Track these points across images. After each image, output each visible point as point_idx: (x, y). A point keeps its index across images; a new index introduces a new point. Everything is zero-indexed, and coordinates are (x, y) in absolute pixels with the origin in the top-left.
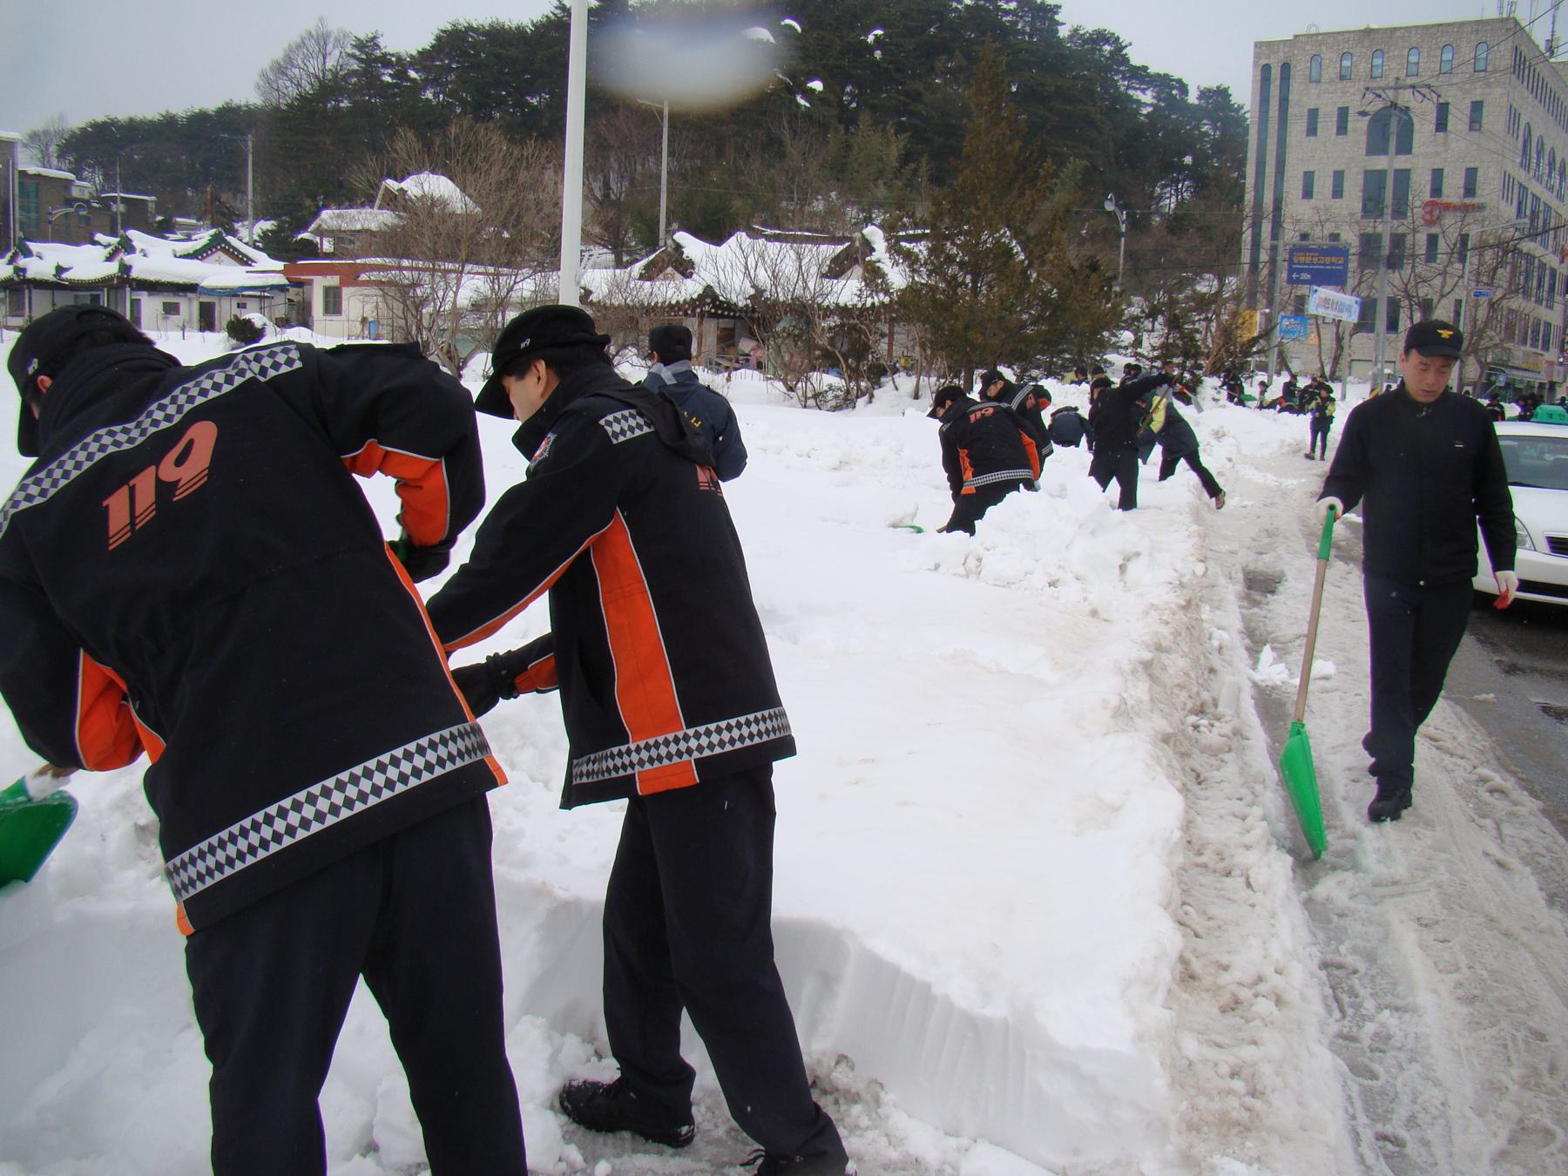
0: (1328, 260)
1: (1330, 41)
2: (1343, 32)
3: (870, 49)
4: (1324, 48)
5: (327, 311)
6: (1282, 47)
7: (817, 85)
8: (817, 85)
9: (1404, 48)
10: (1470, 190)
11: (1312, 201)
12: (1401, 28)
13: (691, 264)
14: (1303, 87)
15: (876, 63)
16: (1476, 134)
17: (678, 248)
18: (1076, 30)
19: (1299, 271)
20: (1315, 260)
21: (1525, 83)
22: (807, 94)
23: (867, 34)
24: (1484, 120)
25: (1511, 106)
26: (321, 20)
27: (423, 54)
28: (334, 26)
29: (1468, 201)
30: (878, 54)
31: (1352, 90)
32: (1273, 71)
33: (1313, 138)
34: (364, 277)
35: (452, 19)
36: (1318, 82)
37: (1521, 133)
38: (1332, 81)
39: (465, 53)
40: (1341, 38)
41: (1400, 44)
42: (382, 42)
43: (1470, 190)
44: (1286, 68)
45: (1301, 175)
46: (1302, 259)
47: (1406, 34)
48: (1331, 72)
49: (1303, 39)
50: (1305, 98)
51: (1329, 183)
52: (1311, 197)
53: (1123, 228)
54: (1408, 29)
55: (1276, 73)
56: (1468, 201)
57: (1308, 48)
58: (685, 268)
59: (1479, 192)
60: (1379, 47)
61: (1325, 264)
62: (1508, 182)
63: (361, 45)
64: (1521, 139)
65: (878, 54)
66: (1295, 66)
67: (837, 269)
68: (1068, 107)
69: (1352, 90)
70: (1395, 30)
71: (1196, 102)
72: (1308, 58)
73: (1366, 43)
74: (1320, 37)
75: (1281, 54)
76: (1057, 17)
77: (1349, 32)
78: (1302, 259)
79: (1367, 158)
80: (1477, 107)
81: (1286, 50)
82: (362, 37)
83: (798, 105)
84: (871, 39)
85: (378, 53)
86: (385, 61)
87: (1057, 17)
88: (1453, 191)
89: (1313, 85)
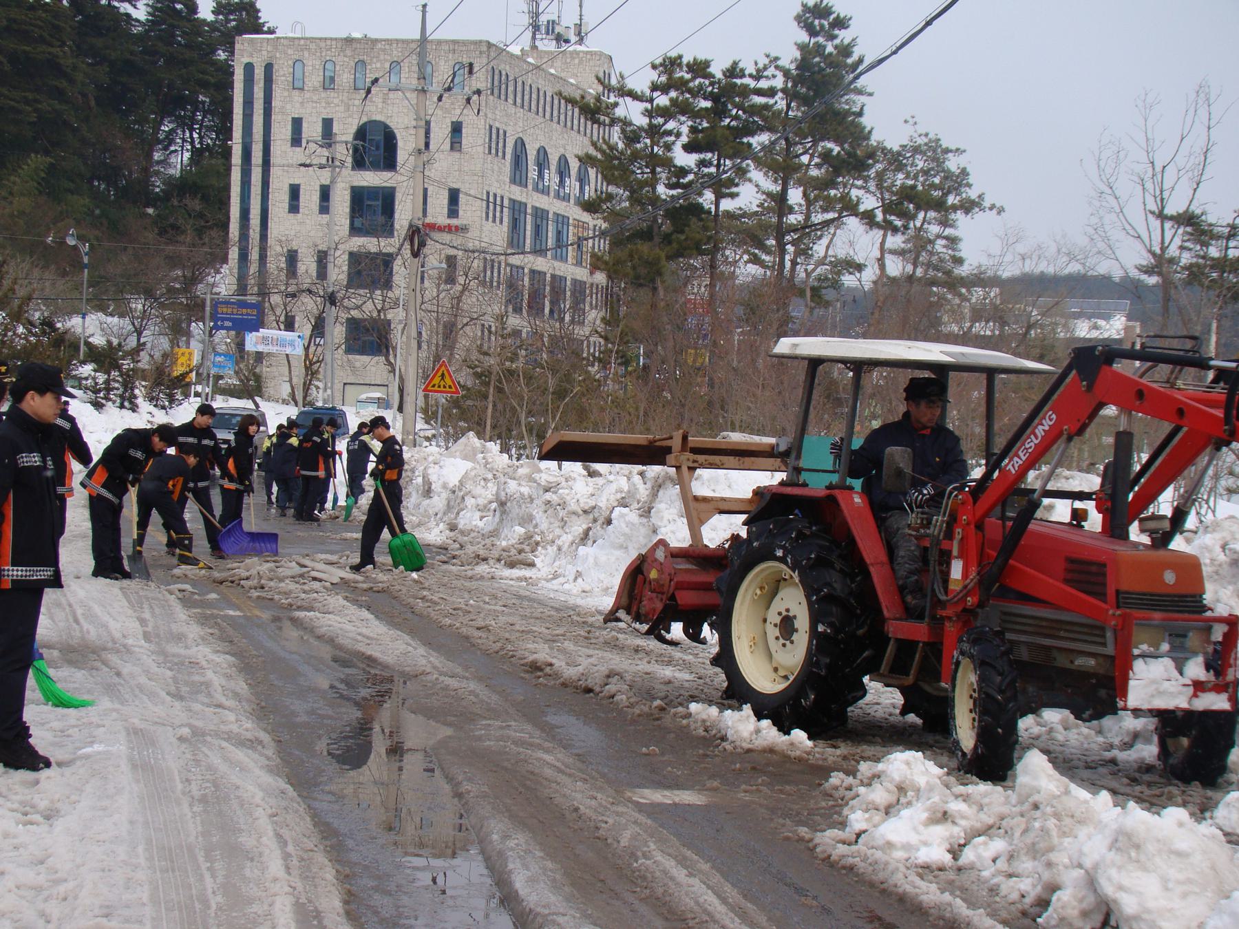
0: (244, 311)
1: (313, 46)
2: (326, 39)
4: (306, 54)
6: (265, 44)
9: (386, 60)
10: (453, 212)
11: (299, 216)
12: (382, 40)
14: (286, 94)
16: (457, 155)
19: (223, 320)
20: (235, 311)
21: (510, 101)
24: (464, 142)
25: (491, 127)
29: (454, 222)
31: (336, 101)
32: (256, 71)
33: (298, 149)
36: (302, 89)
37: (509, 150)
38: (315, 89)
40: (323, 44)
41: (382, 57)
43: (453, 212)
44: (269, 68)
45: (286, 189)
46: (225, 310)
47: (387, 47)
48: (314, 80)
49: (285, 42)
50: (288, 106)
51: (316, 197)
52: (298, 212)
53: (86, 260)
54: (389, 42)
55: (259, 73)
56: (454, 222)
57: (290, 52)
59: (461, 213)
60: (361, 58)
61: (242, 315)
62: (492, 203)
64: (509, 156)
66: (278, 71)
68: (27, 48)
69: (336, 101)
70: (376, 41)
71: (210, 17)
72: (291, 63)
73: (349, 52)
74: (302, 42)
75: (265, 53)
77: (331, 39)
78: (225, 310)
79: (352, 173)
80: (457, 129)
81: (269, 48)
88: (438, 212)
89: (296, 93)
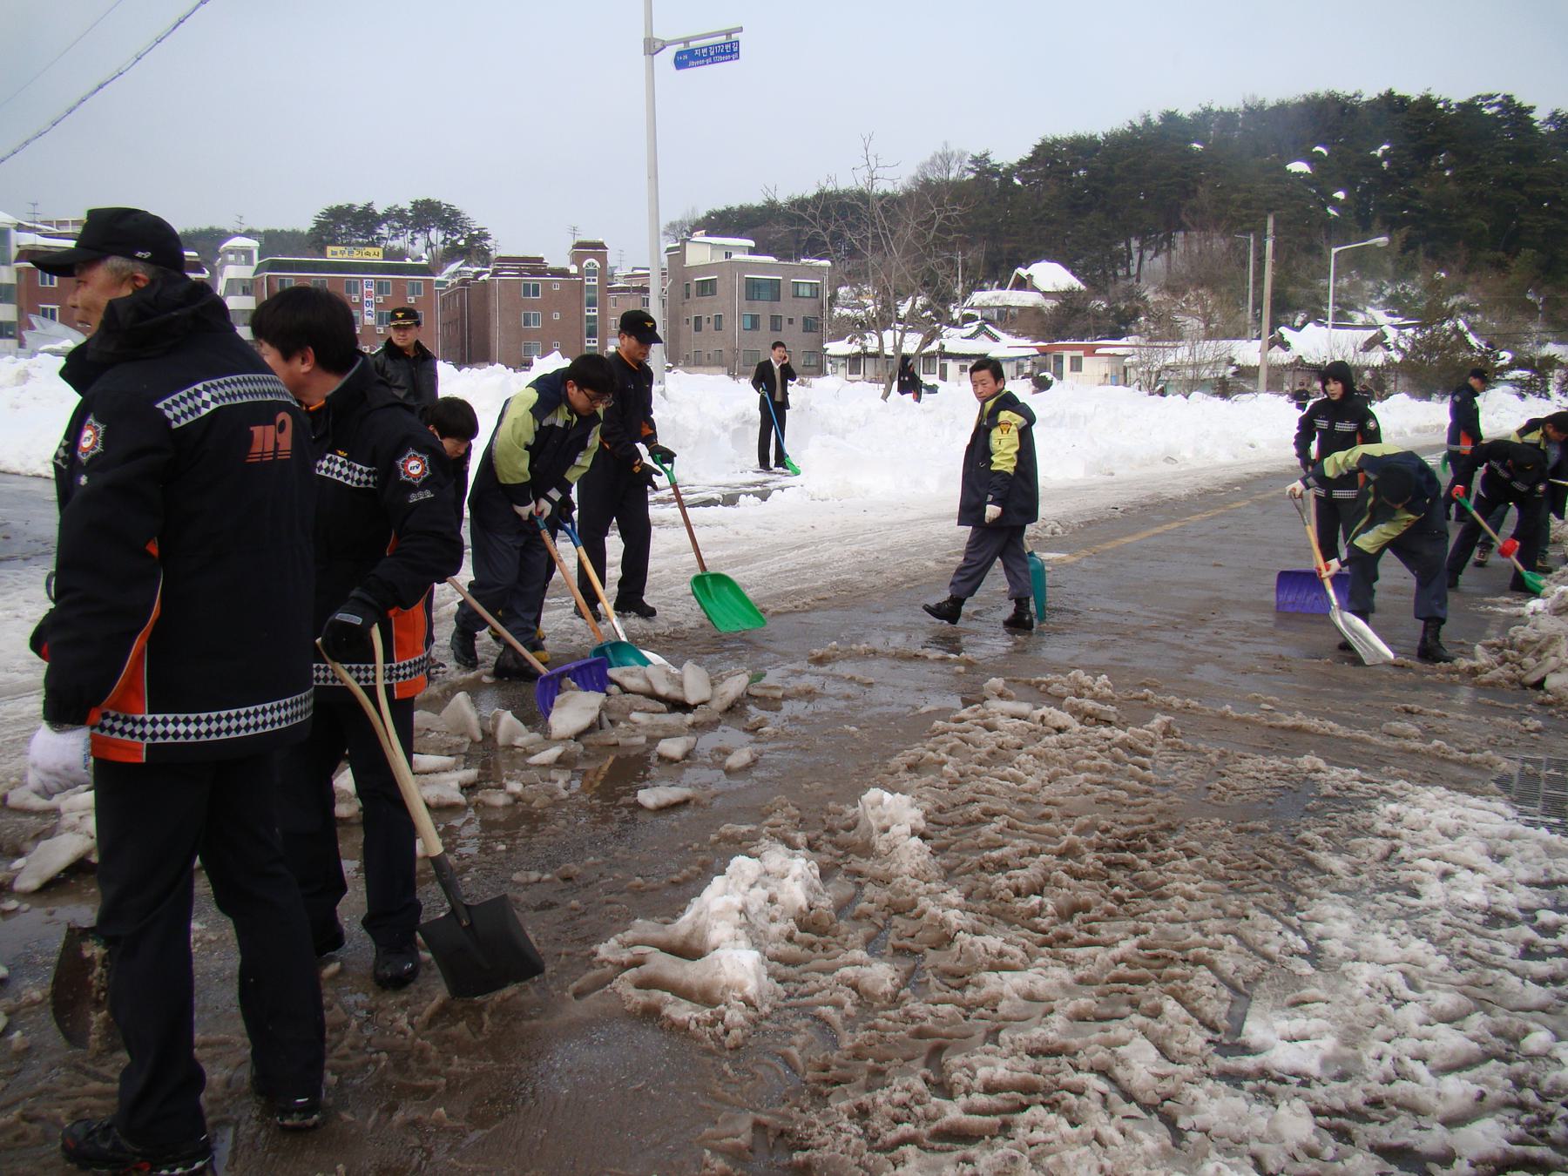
3: (1380, 161)
5: (1072, 370)
7: (1340, 195)
8: (1340, 195)
13: (1288, 344)
15: (1384, 172)
17: (1281, 335)
18: (1555, 114)
22: (1335, 203)
23: (1376, 149)
26: (946, 144)
27: (1022, 163)
28: (954, 147)
30: (1385, 164)
34: (1098, 351)
35: (1042, 135)
39: (1053, 162)
42: (991, 157)
58: (1285, 346)
63: (975, 160)
65: (1385, 164)
67: (1369, 346)
76: (1531, 115)
82: (977, 155)
83: (1329, 215)
84: (1379, 153)
85: (988, 166)
86: (994, 171)
87: (1531, 115)
